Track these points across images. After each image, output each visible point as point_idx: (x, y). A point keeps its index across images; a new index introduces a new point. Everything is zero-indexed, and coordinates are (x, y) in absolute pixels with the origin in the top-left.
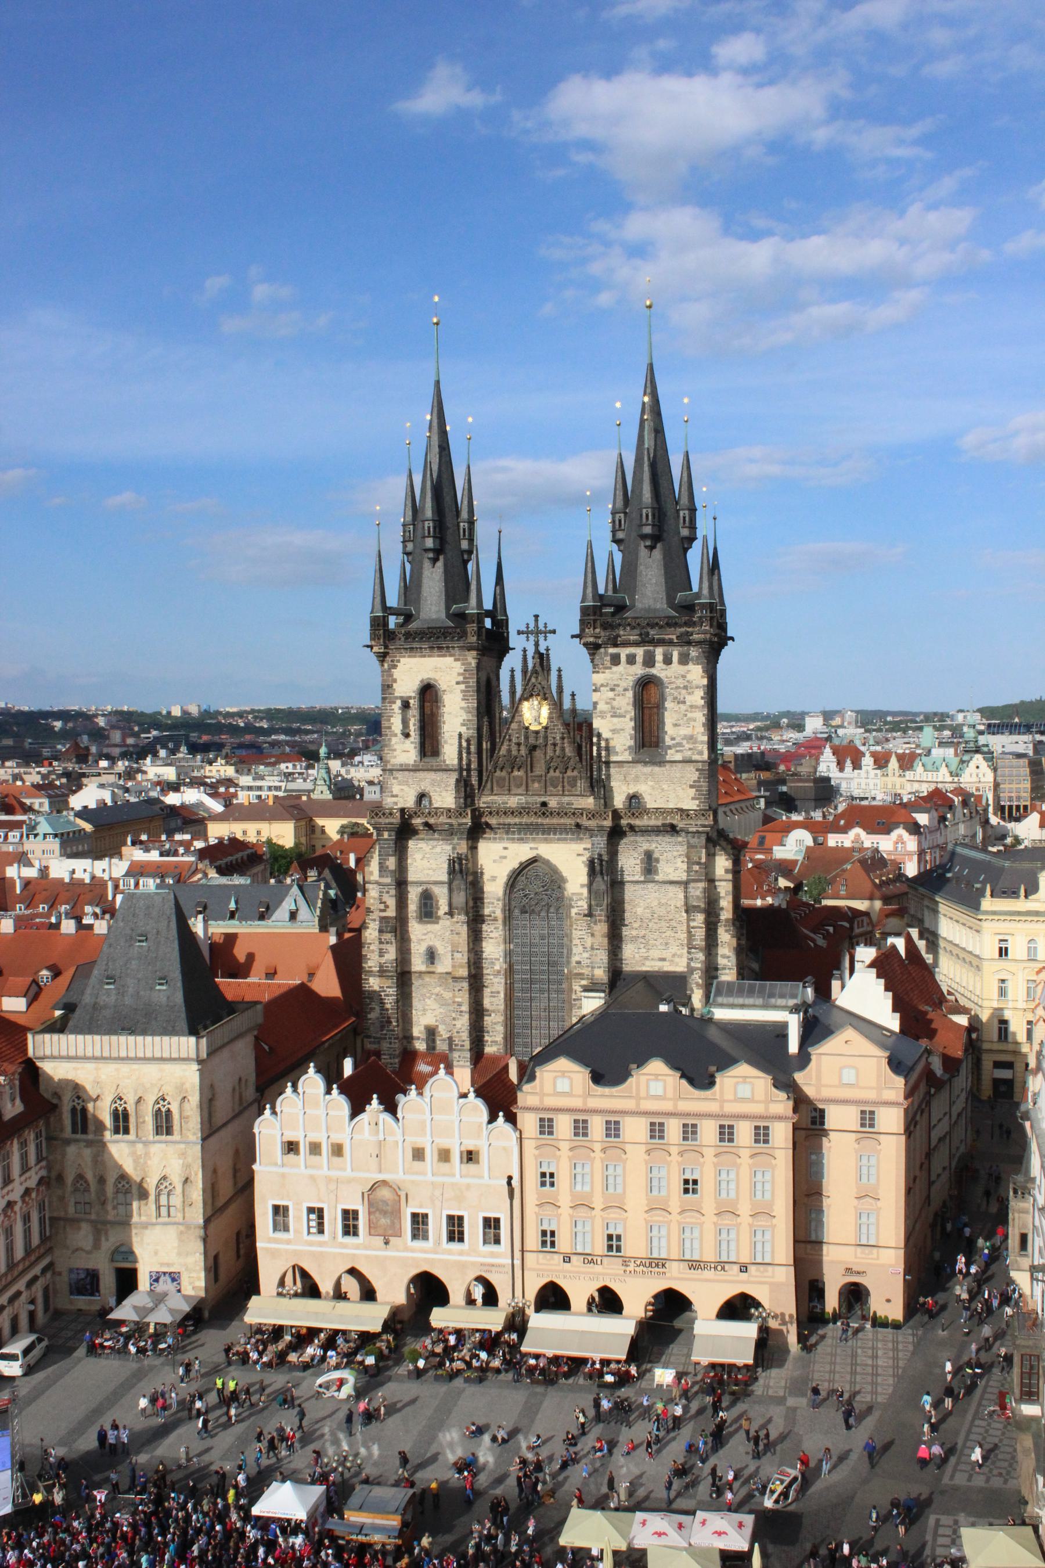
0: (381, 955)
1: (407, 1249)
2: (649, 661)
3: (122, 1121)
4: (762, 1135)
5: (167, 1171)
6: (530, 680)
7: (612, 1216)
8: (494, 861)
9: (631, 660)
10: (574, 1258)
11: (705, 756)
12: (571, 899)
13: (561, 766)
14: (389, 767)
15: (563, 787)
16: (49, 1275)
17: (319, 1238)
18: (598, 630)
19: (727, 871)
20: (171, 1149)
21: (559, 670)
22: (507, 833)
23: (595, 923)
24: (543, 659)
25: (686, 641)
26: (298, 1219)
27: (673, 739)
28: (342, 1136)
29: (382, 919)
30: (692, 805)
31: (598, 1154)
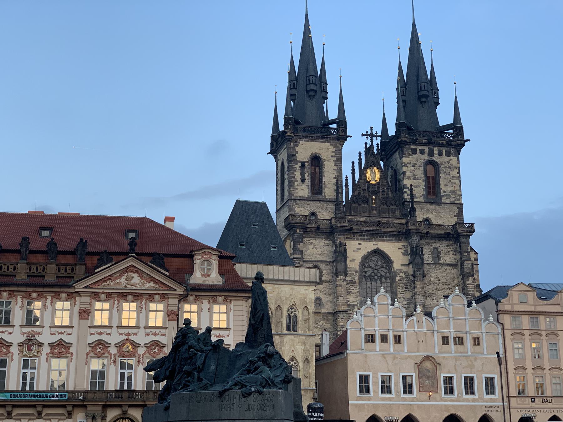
1: (442, 400)
2: (431, 154)
7: (554, 373)
8: (354, 251)
9: (422, 152)
10: (537, 399)
14: (293, 198)
15: (389, 213)
20: (297, 339)
22: (360, 236)
23: (417, 281)
25: (449, 144)
26: (375, 383)
27: (445, 192)
31: (544, 337)
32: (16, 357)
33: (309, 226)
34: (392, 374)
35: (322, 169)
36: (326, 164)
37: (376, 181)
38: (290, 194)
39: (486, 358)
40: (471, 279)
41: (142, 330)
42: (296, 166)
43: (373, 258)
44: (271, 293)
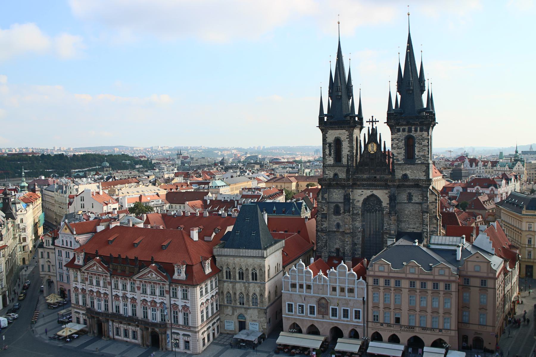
0: (322, 225)
1: (330, 319)
6: (371, 137)
9: (404, 130)
12: (384, 208)
14: (325, 165)
16: (219, 322)
18: (392, 121)
19: (436, 200)
20: (256, 285)
21: (380, 134)
24: (374, 131)
25: (422, 124)
26: (296, 308)
27: (418, 156)
28: (311, 283)
30: (424, 178)
32: (121, 301)
33: (332, 183)
34: (304, 304)
35: (341, 146)
36: (343, 143)
37: (374, 151)
39: (356, 300)
40: (426, 215)
41: (158, 297)
42: (326, 146)
43: (372, 199)
44: (243, 262)
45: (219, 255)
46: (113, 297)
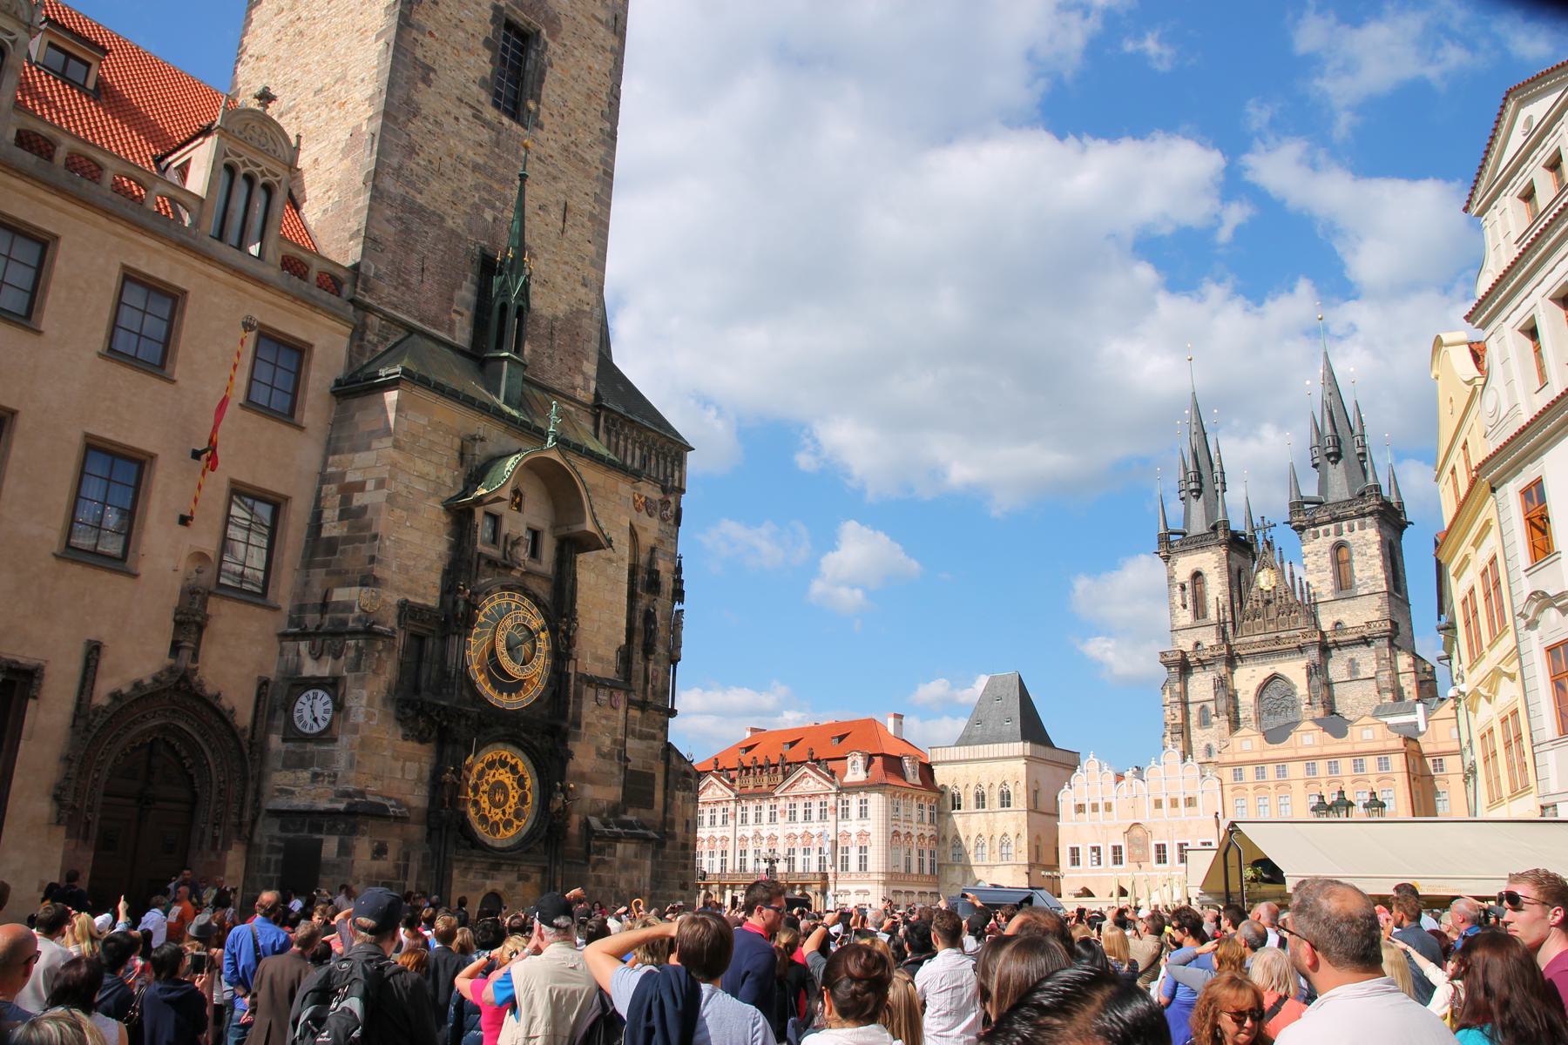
1: (1153, 870)
3: (981, 800)
4: (1383, 764)
5: (1006, 830)
9: (1327, 533)
11: (1385, 589)
13: (1287, 611)
17: (1099, 867)
19: (1409, 665)
26: (1085, 855)
29: (1173, 725)
31: (1273, 789)
38: (1173, 625)
45: (937, 763)
46: (737, 842)
